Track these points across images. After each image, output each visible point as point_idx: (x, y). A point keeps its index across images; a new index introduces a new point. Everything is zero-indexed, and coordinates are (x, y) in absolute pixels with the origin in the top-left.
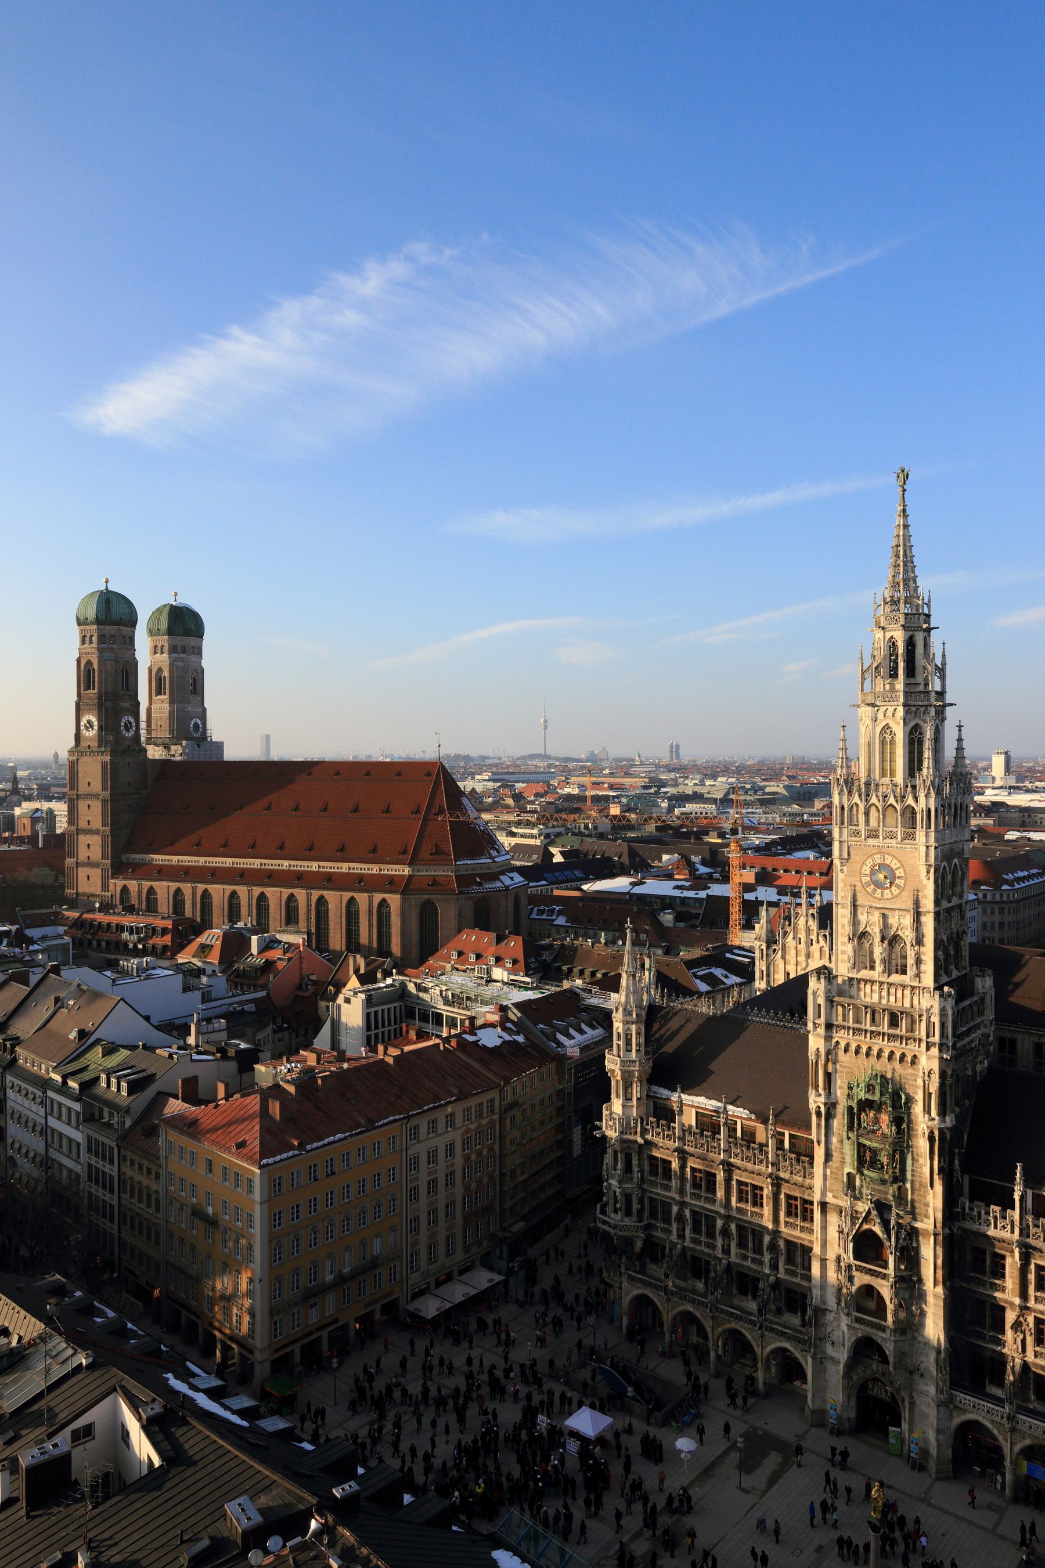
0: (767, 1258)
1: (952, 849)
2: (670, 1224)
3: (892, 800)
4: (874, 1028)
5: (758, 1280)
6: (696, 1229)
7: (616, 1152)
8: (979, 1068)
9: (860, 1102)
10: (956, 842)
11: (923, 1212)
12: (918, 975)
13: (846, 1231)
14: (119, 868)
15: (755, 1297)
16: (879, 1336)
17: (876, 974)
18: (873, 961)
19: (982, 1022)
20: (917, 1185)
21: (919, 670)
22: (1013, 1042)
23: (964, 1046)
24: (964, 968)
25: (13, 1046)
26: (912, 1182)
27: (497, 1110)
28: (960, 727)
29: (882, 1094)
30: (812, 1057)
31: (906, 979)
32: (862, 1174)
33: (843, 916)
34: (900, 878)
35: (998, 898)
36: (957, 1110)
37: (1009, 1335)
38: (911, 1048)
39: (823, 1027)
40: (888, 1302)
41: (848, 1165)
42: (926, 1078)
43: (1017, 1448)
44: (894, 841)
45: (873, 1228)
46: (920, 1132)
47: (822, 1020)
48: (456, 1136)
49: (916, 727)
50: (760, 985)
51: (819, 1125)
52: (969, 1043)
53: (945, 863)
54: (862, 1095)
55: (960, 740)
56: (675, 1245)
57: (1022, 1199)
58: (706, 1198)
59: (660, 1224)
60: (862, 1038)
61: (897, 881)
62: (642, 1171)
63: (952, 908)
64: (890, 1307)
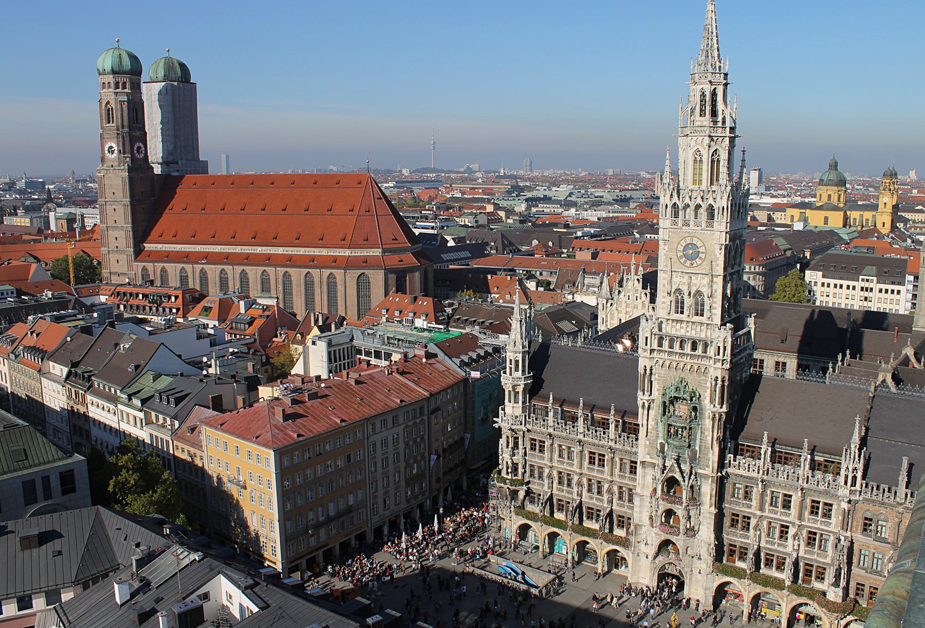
0: (606, 497)
3: (699, 201)
6: (560, 483)
8: (744, 375)
14: (138, 252)
15: (597, 521)
16: (673, 539)
18: (682, 308)
20: (703, 448)
25: (90, 377)
26: (700, 446)
27: (426, 412)
30: (641, 370)
31: (704, 319)
35: (752, 270)
38: (705, 362)
42: (714, 383)
43: (752, 595)
48: (400, 429)
50: (602, 328)
54: (673, 394)
55: (743, 160)
56: (547, 493)
59: (536, 481)
60: (673, 358)
63: (733, 273)
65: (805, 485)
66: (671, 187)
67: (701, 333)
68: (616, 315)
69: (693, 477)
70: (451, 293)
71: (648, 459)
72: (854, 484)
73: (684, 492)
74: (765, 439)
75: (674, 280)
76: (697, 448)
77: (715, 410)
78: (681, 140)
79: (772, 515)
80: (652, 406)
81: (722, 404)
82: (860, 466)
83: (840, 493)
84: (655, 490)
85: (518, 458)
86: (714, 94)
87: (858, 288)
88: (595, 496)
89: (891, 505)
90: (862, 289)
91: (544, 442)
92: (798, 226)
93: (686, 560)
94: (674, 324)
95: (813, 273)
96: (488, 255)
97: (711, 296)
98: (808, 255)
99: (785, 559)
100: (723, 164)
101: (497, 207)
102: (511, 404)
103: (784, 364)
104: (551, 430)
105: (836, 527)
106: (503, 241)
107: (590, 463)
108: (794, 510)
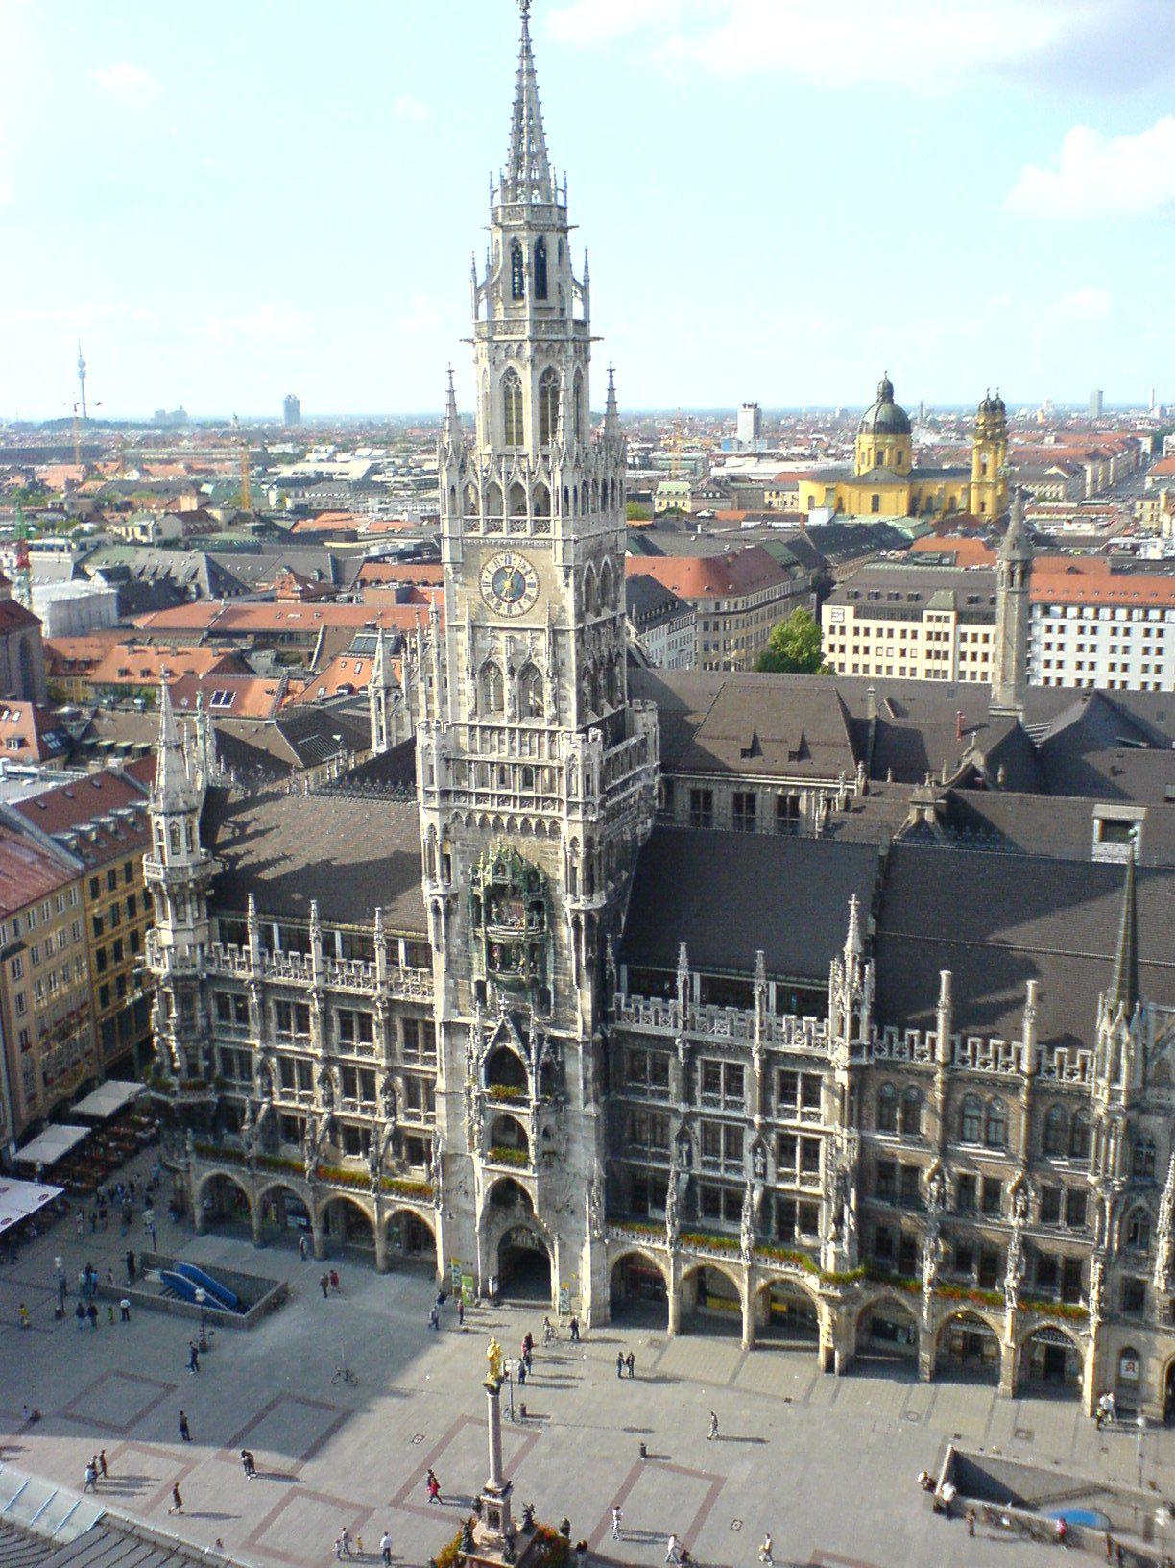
0: (381, 1101)
2: (251, 1079)
8: (640, 830)
9: (487, 888)
12: (557, 718)
15: (366, 1154)
21: (552, 289)
22: (708, 795)
24: (622, 702)
29: (514, 875)
30: (424, 835)
32: (493, 979)
34: (531, 585)
36: (611, 885)
37: (674, 1146)
40: (529, 1132)
44: (521, 535)
47: (435, 788)
49: (549, 372)
50: (378, 748)
51: (437, 925)
55: (611, 390)
57: (688, 985)
60: (487, 806)
61: (528, 590)
62: (208, 1016)
64: (532, 1137)
76: (550, 987)
77: (577, 906)
82: (867, 996)
87: (922, 635)
90: (930, 636)
95: (838, 609)
97: (557, 672)
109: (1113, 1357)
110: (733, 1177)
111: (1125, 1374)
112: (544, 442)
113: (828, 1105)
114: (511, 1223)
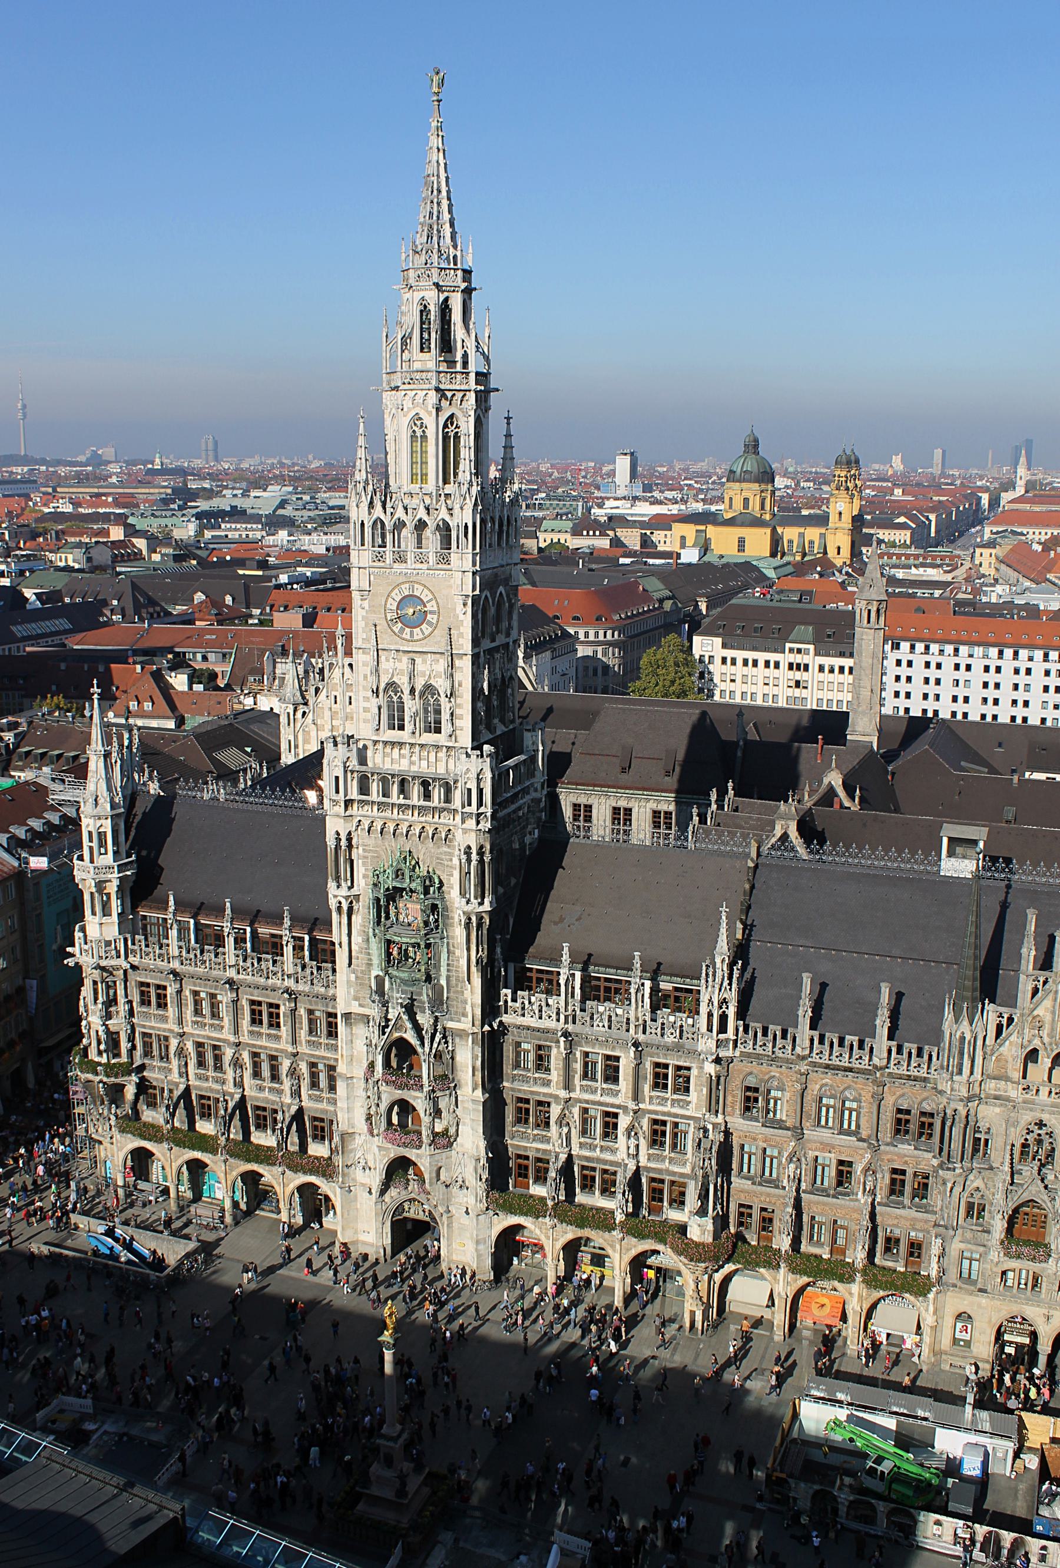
0: (287, 1084)
1: (496, 575)
3: (422, 514)
4: (402, 801)
5: (275, 1111)
7: (95, 983)
8: (528, 839)
10: (502, 566)
11: (460, 1010)
13: (374, 1042)
16: (412, 1154)
17: (404, 736)
18: (402, 719)
19: (532, 784)
20: (453, 981)
23: (509, 814)
24: (513, 721)
26: (448, 978)
28: (508, 418)
30: (331, 842)
31: (441, 739)
33: (365, 664)
35: (601, 638)
36: (501, 890)
37: (554, 1127)
39: (343, 805)
40: (422, 1115)
41: (375, 966)
42: (464, 857)
43: (560, 1244)
44: (424, 566)
45: (405, 1036)
46: (456, 920)
50: (287, 759)
52: (514, 812)
53: (487, 593)
54: (391, 884)
55: (508, 436)
56: (177, 1085)
58: (212, 1025)
59: (156, 1063)
60: (388, 814)
61: (429, 617)
63: (496, 649)
64: (426, 1120)
65: (641, 1037)
66: (370, 488)
67: (438, 766)
68: (313, 734)
69: (438, 1036)
70: (26, 701)
71: (355, 1008)
72: (723, 1029)
73: (425, 1067)
74: (566, 958)
75: (384, 665)
76: (443, 982)
78: (388, 397)
79: (587, 1096)
80: (355, 908)
81: (483, 898)
82: (732, 996)
83: (701, 1046)
84: (372, 1065)
85: (118, 1023)
86: (445, 309)
87: (784, 666)
88: (267, 1084)
89: (787, 1061)
90: (791, 666)
91: (165, 988)
92: (690, 556)
93: (437, 1192)
94: (388, 749)
95: (707, 640)
96: (106, 624)
98: (703, 607)
99: (615, 1173)
100: (468, 441)
101: (132, 531)
102: (97, 919)
103: (628, 811)
104: (175, 965)
105: (697, 1108)
106: (135, 600)
107: (253, 1021)
108: (625, 1083)
109: (949, 1320)
110: (607, 1156)
111: (958, 1335)
112: (446, 481)
113: (697, 1094)
114: (404, 1195)
